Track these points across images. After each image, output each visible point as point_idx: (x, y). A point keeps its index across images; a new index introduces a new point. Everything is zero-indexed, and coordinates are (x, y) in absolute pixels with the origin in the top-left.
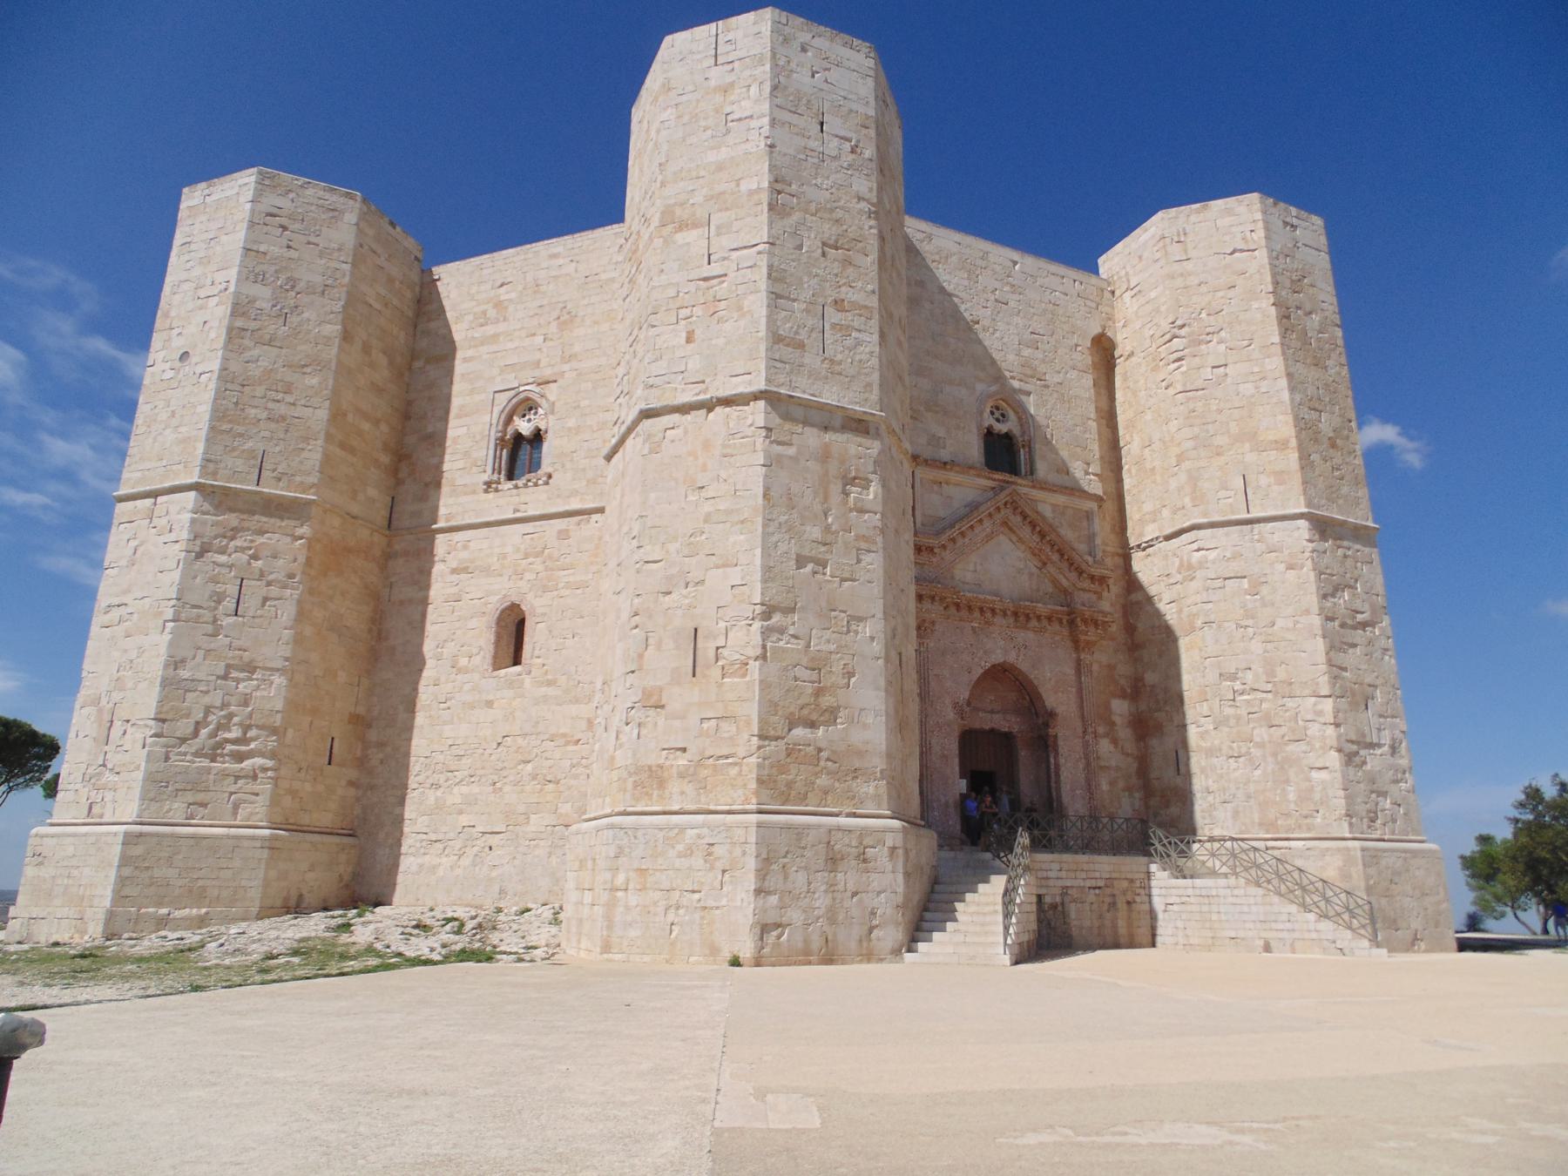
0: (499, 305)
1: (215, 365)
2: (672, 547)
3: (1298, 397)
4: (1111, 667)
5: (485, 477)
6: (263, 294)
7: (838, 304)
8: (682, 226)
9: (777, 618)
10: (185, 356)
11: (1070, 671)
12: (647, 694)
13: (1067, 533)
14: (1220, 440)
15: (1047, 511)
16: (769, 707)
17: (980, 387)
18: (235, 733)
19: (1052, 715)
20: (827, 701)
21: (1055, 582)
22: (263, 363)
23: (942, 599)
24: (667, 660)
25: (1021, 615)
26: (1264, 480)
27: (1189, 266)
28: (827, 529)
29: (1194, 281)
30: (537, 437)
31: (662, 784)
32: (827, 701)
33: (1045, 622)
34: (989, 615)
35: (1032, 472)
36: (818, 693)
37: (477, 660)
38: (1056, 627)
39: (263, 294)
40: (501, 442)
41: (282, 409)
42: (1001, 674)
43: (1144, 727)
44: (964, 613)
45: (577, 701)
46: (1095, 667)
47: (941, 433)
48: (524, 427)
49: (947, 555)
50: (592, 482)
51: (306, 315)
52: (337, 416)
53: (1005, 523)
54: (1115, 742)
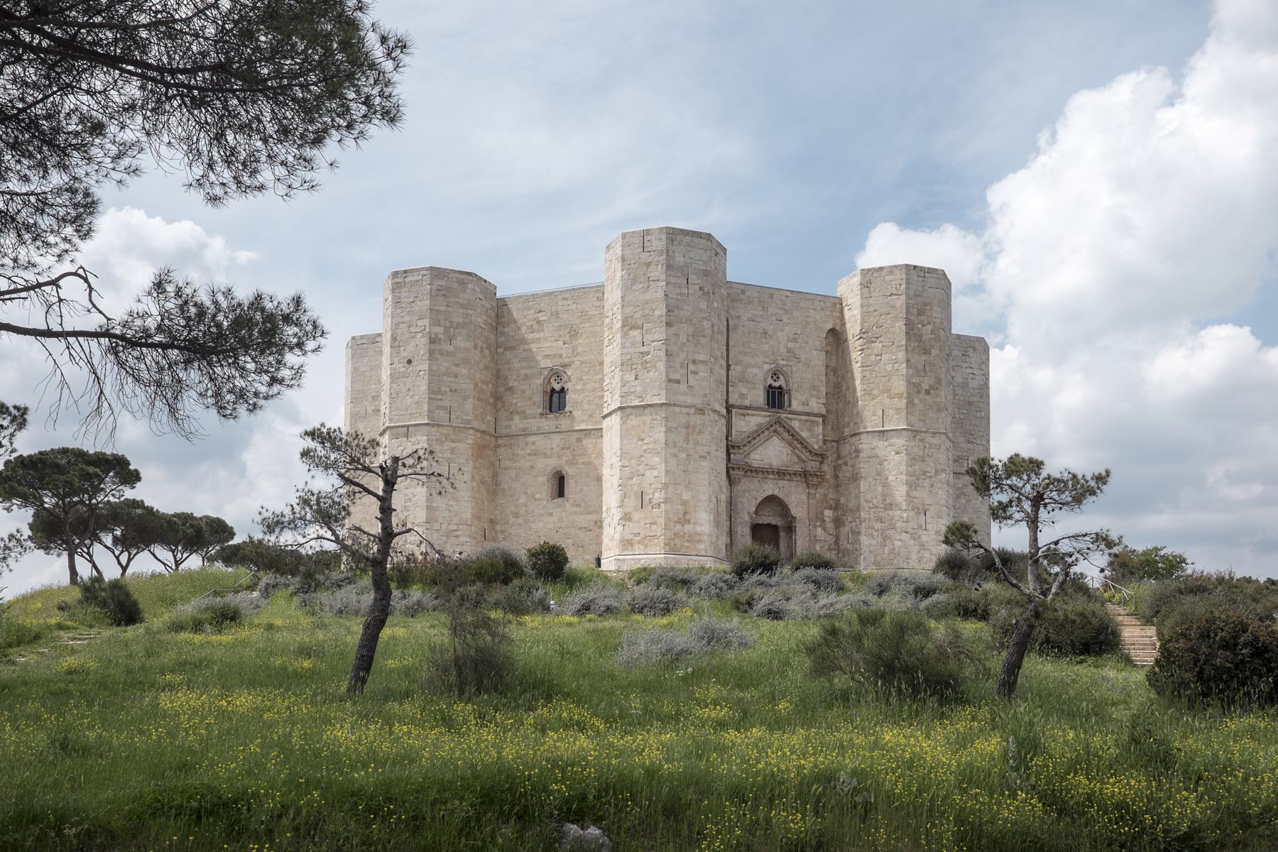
0: (539, 322)
1: (426, 367)
2: (633, 461)
3: (911, 372)
4: (825, 495)
5: (540, 411)
6: (440, 330)
7: (694, 362)
8: (633, 328)
9: (671, 489)
10: (409, 362)
11: (805, 498)
12: (626, 514)
13: (804, 434)
14: (875, 392)
15: (796, 424)
16: (668, 519)
17: (766, 367)
18: (453, 527)
19: (794, 518)
20: (688, 517)
21: (799, 457)
22: (445, 364)
24: (632, 503)
25: (781, 474)
26: (891, 412)
27: (871, 301)
28: (688, 455)
29: (872, 309)
30: (563, 389)
31: (632, 545)
32: (688, 517)
36: (685, 513)
37: (544, 495)
39: (440, 330)
40: (545, 392)
41: (454, 386)
42: (771, 500)
43: (838, 522)
45: (589, 513)
47: (745, 391)
48: (557, 387)
50: (591, 416)
51: (459, 338)
52: (476, 385)
53: (775, 431)
54: (824, 529)
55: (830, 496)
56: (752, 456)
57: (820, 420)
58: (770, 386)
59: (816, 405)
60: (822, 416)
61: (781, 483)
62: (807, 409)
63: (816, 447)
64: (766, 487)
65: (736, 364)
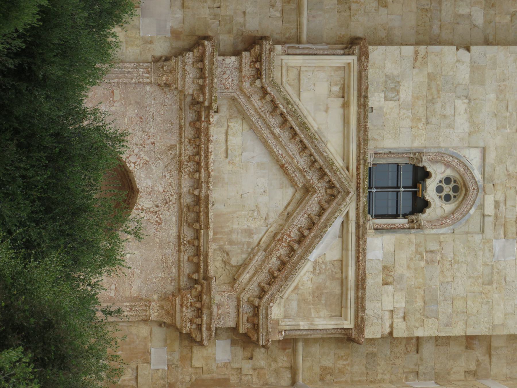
17: (473, 157)
23: (202, 88)
33: (191, 250)
34: (191, 167)
35: (378, 230)
38: (187, 268)
44: (188, 132)
46: (144, 330)
47: (406, 93)
49: (255, 99)
53: (307, 190)
55: (144, 371)
56: (237, 126)
57: (348, 323)
58: (427, 175)
59: (386, 309)
60: (360, 324)
61: (170, 216)
62: (373, 281)
63: (276, 312)
64: (157, 169)
65: (474, 67)
